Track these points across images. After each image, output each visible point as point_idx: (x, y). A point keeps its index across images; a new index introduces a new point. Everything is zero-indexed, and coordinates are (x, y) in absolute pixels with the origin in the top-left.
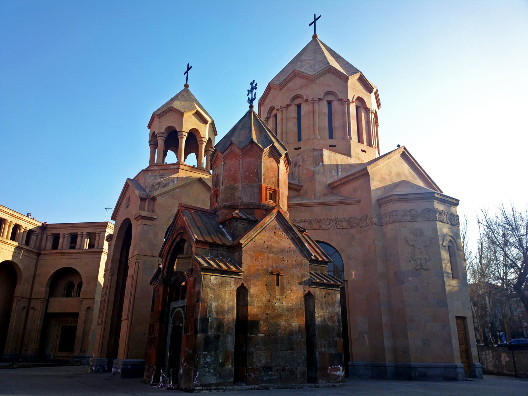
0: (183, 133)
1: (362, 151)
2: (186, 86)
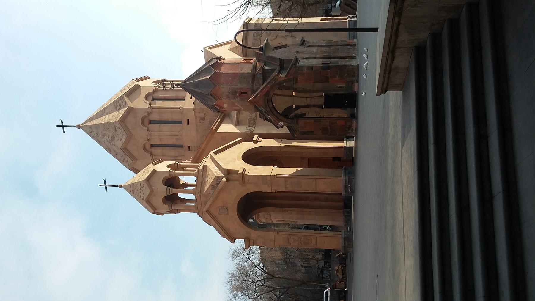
2: (121, 186)
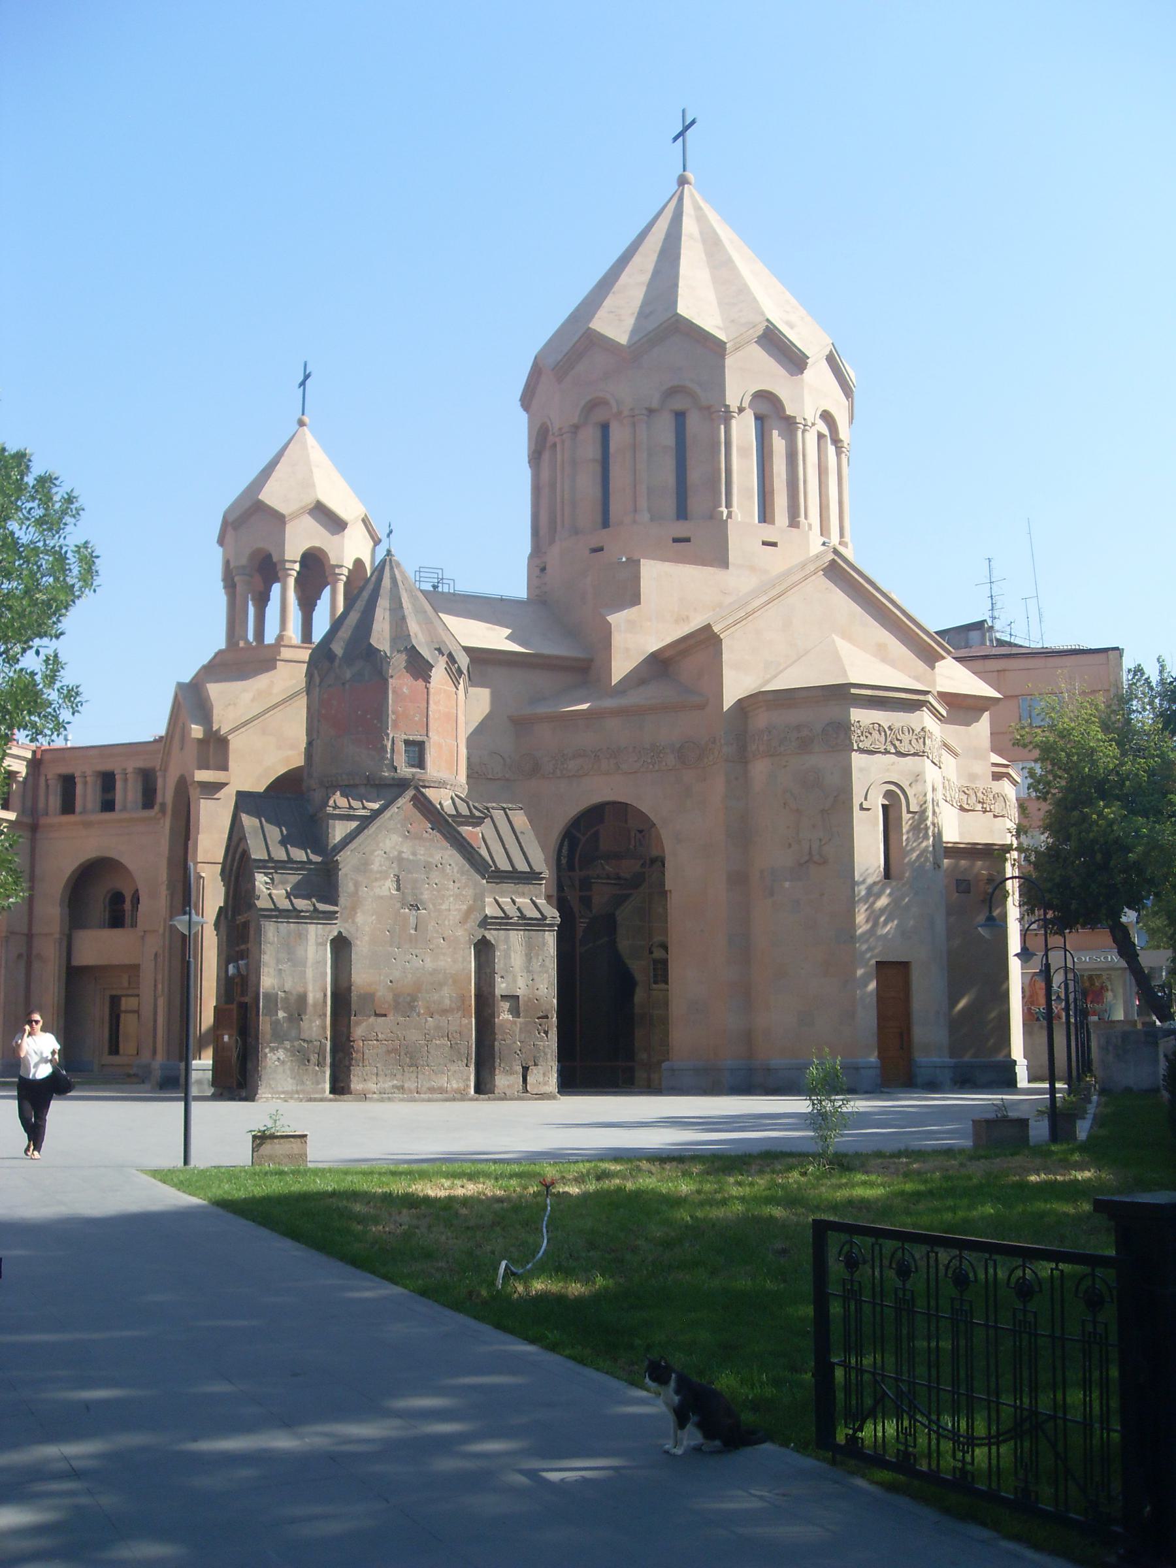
0: (288, 565)
1: (765, 543)
